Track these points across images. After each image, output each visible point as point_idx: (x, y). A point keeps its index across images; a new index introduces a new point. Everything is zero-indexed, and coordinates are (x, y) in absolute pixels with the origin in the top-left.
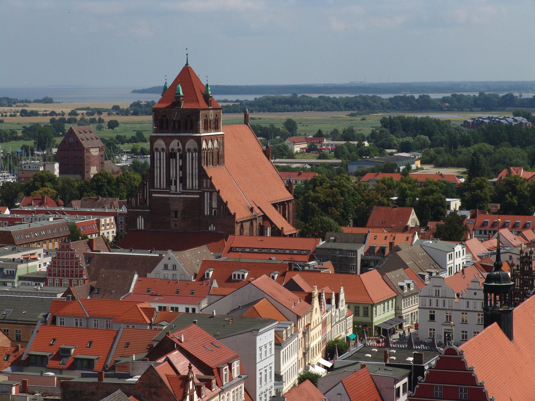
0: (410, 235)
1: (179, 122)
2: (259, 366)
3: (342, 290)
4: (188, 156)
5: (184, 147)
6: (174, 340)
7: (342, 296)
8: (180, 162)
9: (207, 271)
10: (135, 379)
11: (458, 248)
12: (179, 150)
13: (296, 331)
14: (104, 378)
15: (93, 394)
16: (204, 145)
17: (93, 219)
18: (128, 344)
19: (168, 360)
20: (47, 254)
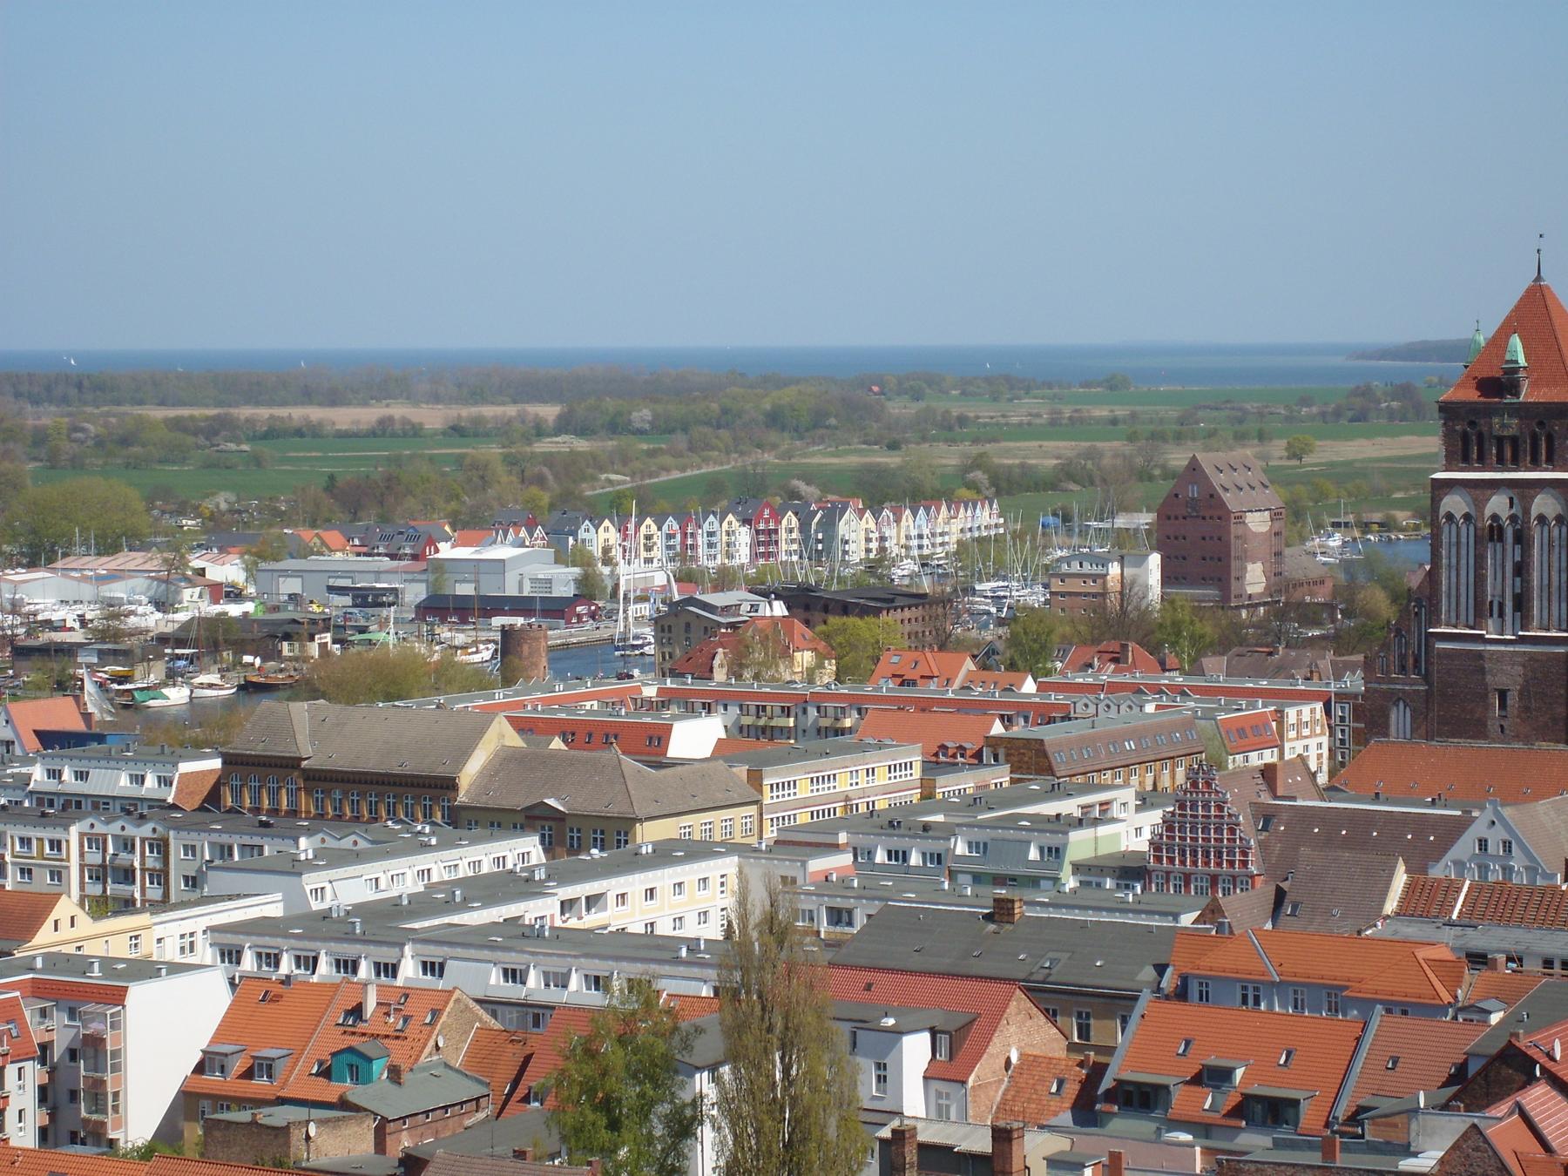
5: (1527, 511)
6: (1531, 1052)
8: (1512, 553)
12: (1513, 518)
17: (1262, 708)
18: (1396, 1061)
20: (1145, 802)
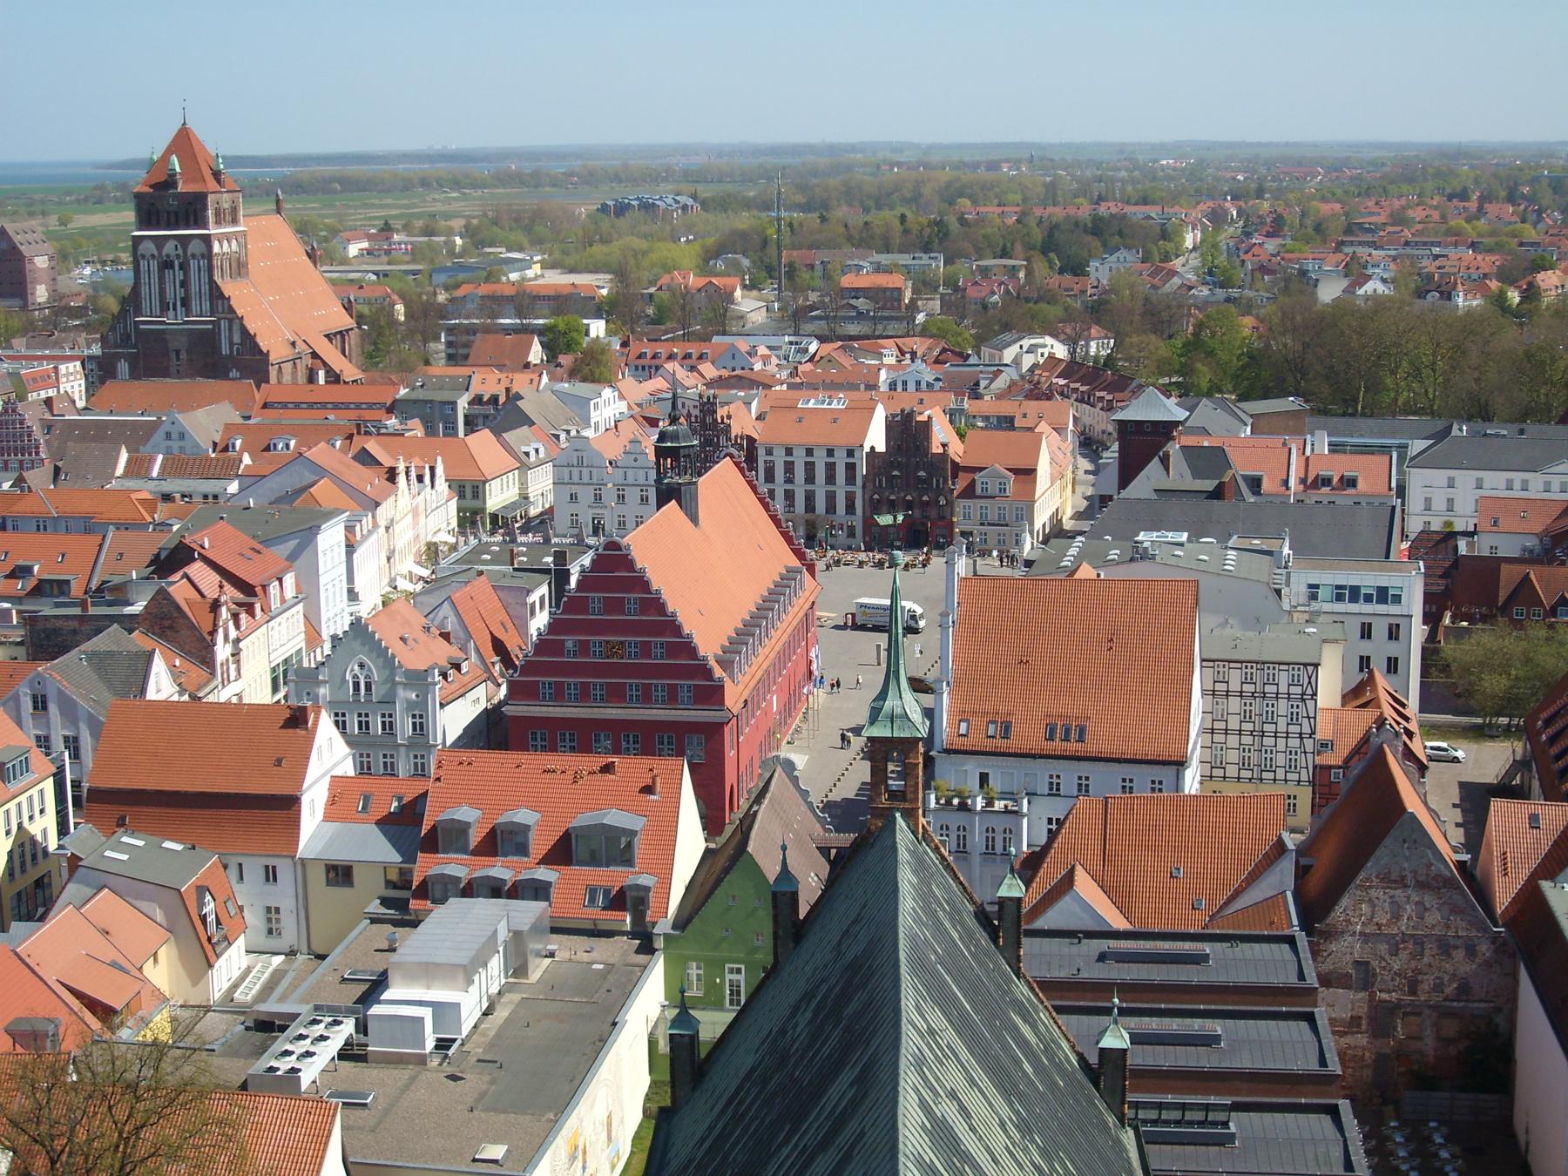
0: (535, 376)
1: (176, 213)
2: (322, 581)
3: (439, 459)
4: (193, 264)
5: (185, 251)
6: (193, 545)
7: (440, 471)
8: (180, 276)
9: (232, 441)
10: (137, 608)
11: (607, 393)
12: (178, 256)
13: (376, 525)
14: (90, 608)
15: (75, 632)
16: (216, 248)
17: (47, 366)
18: (121, 555)
19: (186, 576)
